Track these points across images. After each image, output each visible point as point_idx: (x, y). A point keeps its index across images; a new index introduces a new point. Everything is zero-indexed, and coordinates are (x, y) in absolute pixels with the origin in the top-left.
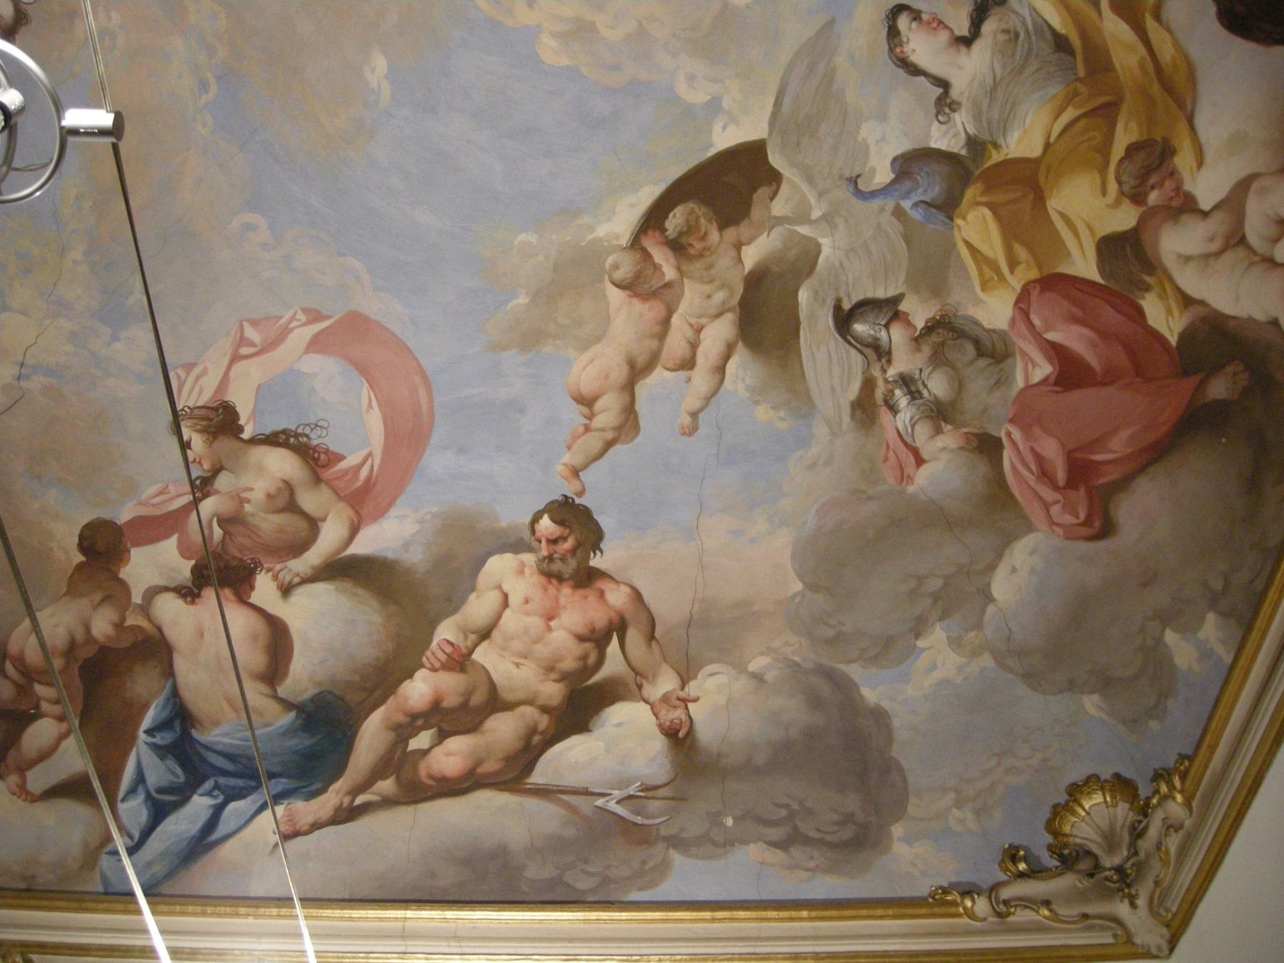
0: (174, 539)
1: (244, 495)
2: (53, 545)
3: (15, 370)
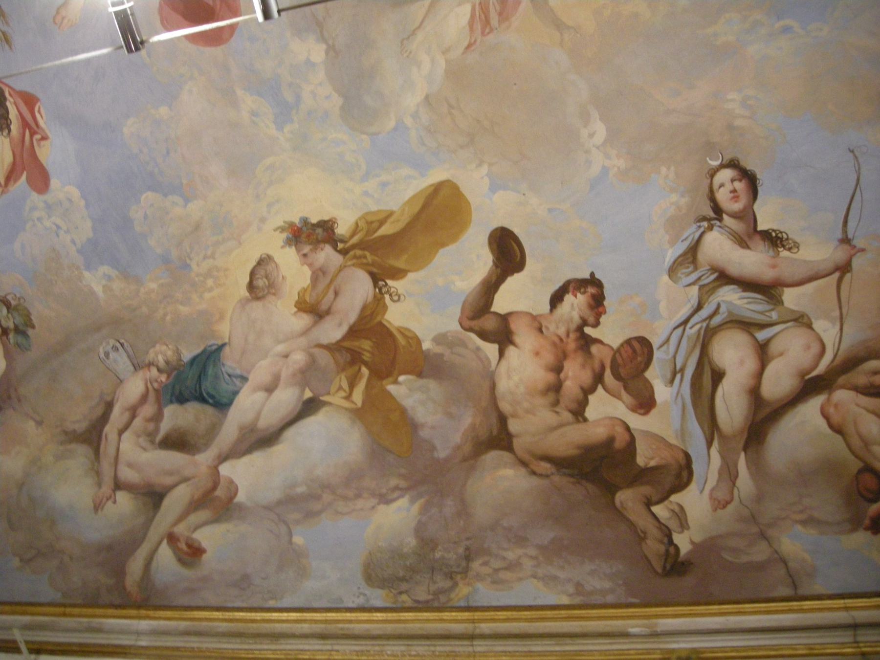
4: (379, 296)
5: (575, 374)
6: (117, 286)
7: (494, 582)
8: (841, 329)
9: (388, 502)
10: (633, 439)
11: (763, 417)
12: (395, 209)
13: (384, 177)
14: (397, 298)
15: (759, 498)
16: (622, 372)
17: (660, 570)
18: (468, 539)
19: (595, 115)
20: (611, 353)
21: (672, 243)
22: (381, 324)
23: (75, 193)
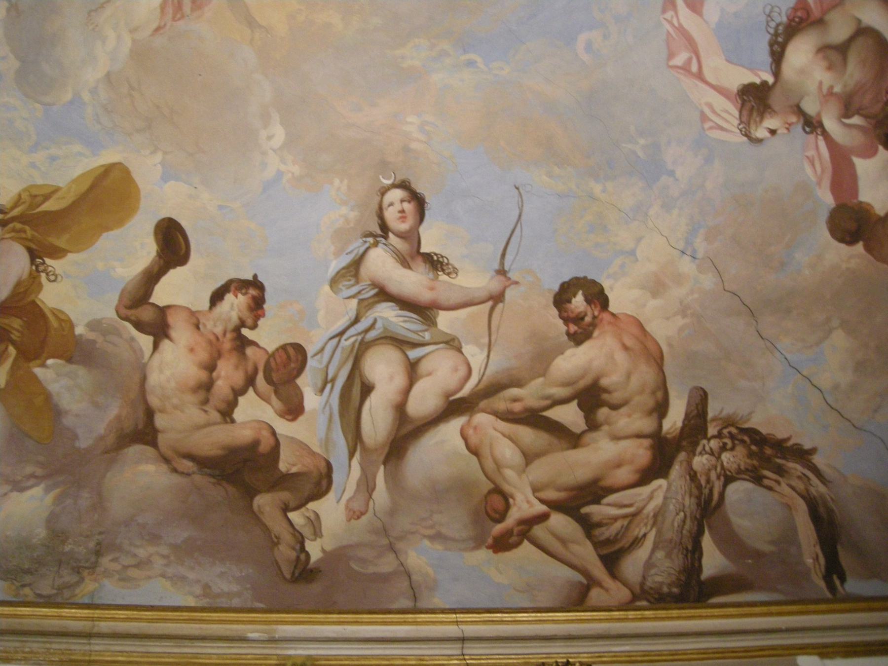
0: (856, 160)
1: (825, 89)
2: (844, 266)
3: (687, 259)
4: (35, 274)
5: (228, 374)
7: (121, 580)
8: (488, 356)
9: (22, 490)
10: (277, 444)
11: (407, 432)
12: (61, 185)
13: (54, 151)
14: (54, 278)
15: (393, 512)
16: (275, 377)
17: (288, 576)
18: (100, 533)
19: (276, 117)
20: (265, 357)
21: (338, 254)
22: (34, 303)
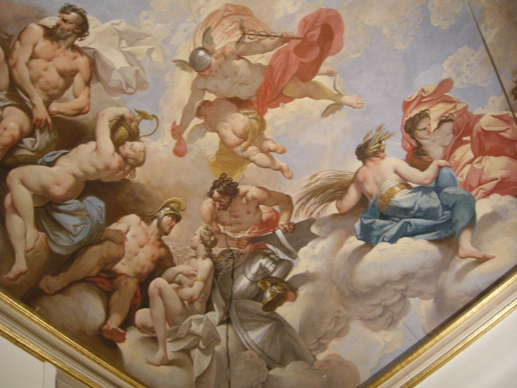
6: (489, 21)
23: (446, 63)
